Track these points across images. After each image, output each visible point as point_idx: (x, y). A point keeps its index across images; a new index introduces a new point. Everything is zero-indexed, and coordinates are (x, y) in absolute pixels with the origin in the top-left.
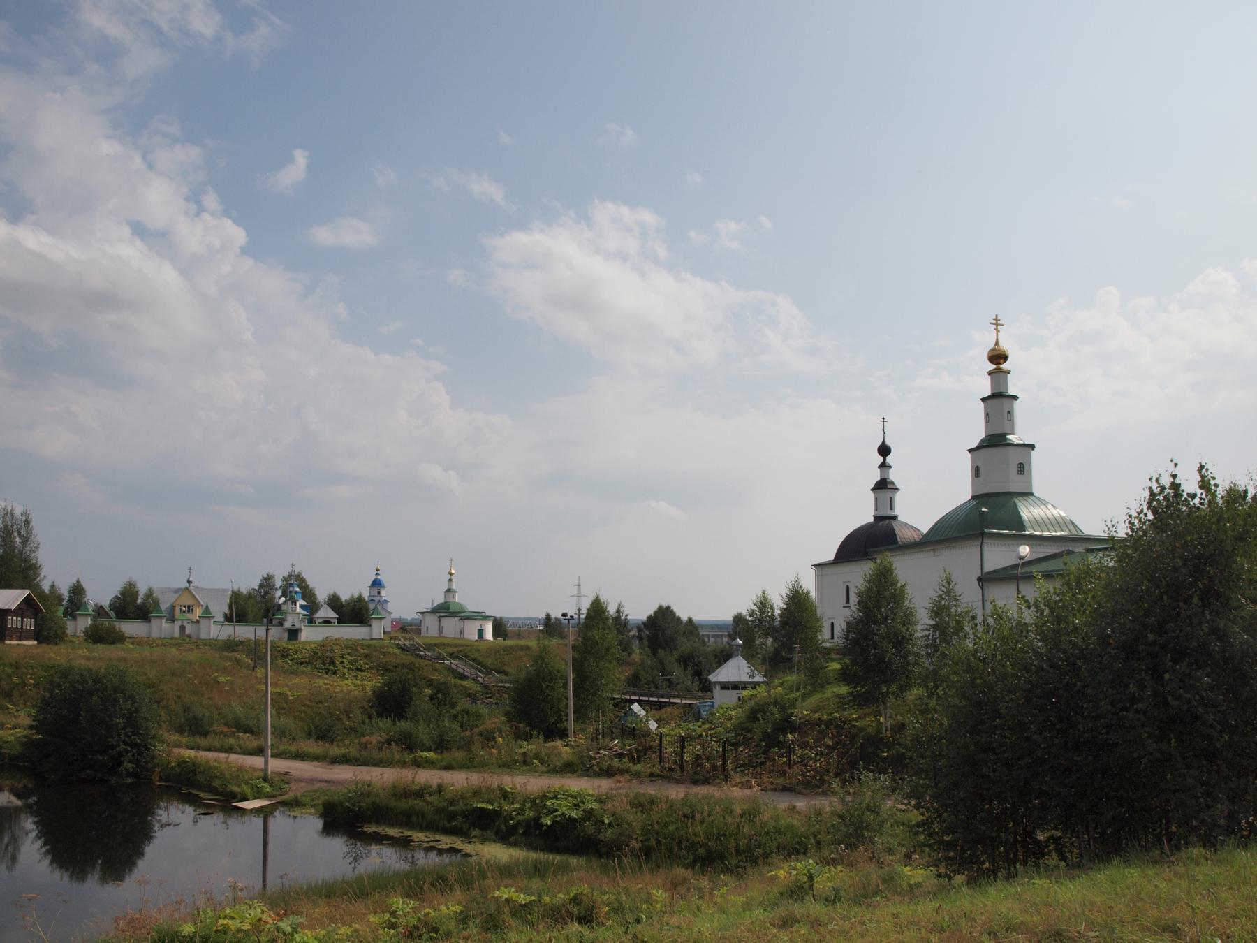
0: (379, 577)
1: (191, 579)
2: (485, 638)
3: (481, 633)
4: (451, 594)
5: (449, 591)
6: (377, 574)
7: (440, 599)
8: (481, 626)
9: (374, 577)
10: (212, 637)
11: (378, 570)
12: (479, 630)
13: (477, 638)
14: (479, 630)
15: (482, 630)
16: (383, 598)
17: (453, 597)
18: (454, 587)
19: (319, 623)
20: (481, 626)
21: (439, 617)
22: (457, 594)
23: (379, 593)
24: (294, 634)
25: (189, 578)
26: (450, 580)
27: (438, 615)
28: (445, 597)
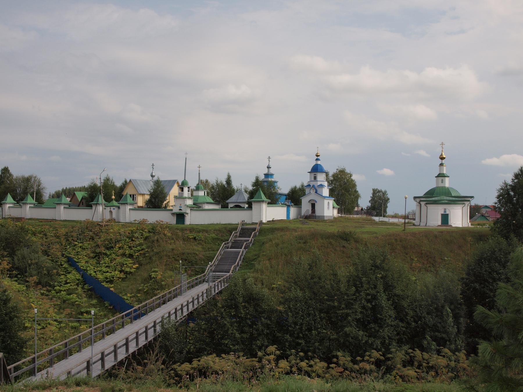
0: (319, 162)
1: (154, 174)
2: (450, 224)
3: (445, 218)
4: (440, 179)
5: (441, 176)
6: (317, 160)
7: (432, 184)
8: (445, 211)
9: (314, 163)
10: (94, 220)
11: (317, 156)
12: (442, 215)
13: (440, 223)
14: (442, 215)
15: (447, 215)
16: (319, 183)
17: (442, 182)
18: (445, 172)
19: (231, 208)
20: (445, 211)
21: (419, 203)
22: (447, 179)
23: (315, 178)
24: (180, 217)
25: (152, 173)
26: (441, 165)
27: (418, 200)
28: (437, 182)
